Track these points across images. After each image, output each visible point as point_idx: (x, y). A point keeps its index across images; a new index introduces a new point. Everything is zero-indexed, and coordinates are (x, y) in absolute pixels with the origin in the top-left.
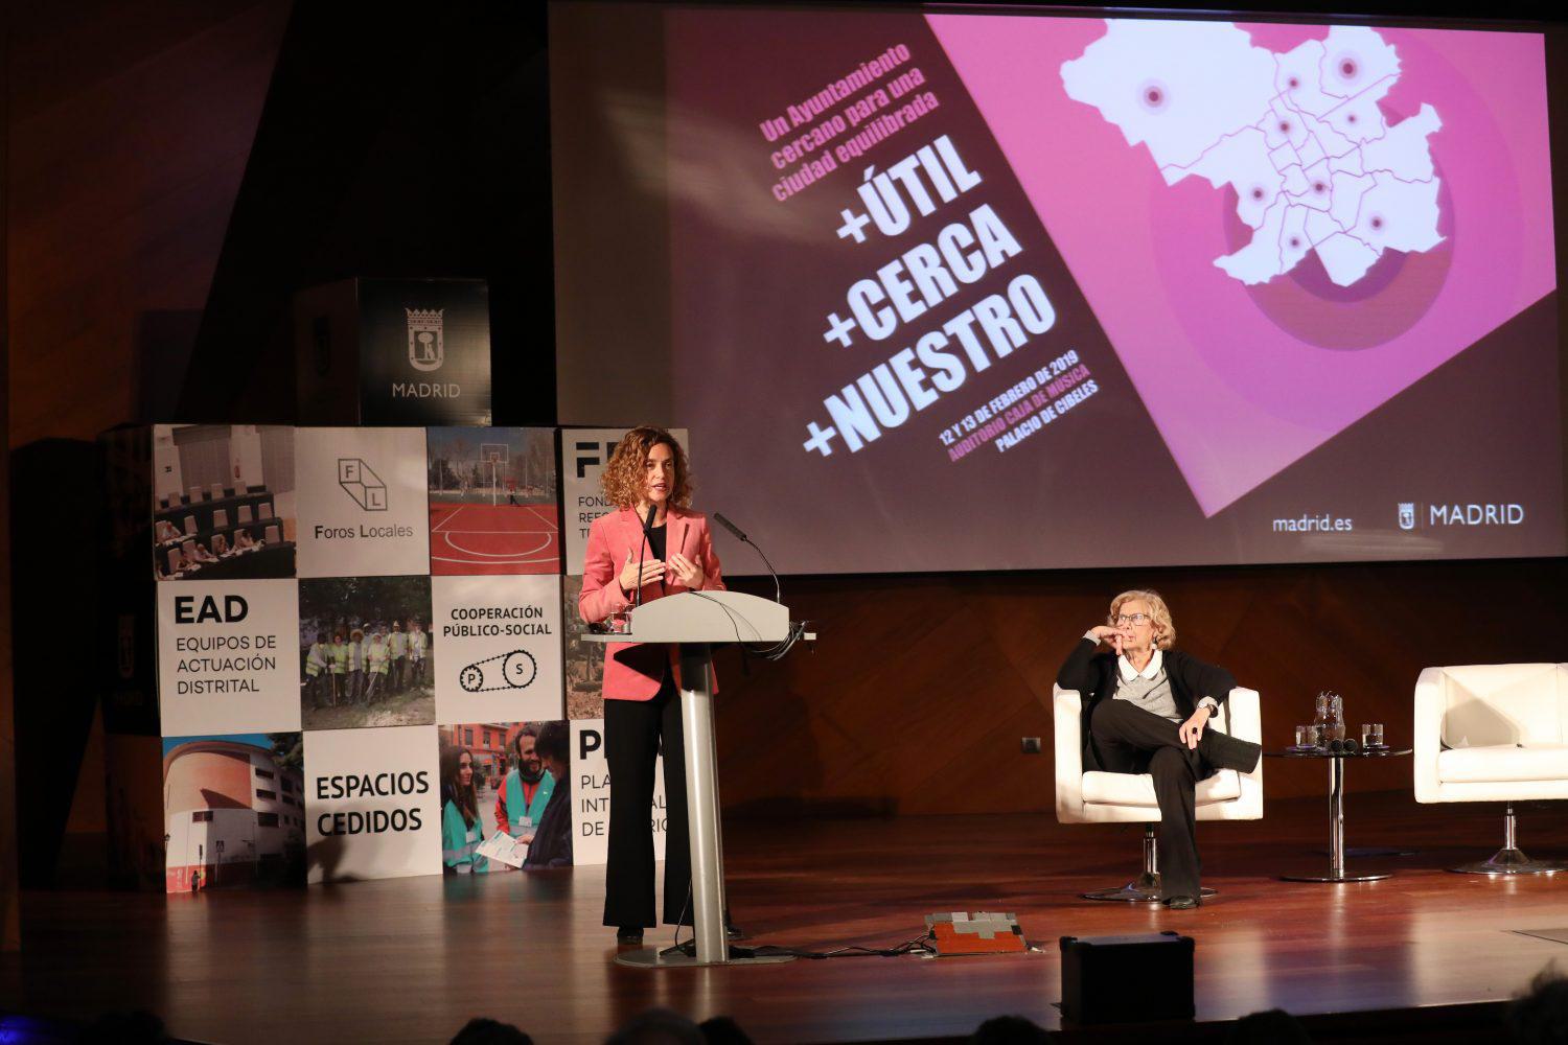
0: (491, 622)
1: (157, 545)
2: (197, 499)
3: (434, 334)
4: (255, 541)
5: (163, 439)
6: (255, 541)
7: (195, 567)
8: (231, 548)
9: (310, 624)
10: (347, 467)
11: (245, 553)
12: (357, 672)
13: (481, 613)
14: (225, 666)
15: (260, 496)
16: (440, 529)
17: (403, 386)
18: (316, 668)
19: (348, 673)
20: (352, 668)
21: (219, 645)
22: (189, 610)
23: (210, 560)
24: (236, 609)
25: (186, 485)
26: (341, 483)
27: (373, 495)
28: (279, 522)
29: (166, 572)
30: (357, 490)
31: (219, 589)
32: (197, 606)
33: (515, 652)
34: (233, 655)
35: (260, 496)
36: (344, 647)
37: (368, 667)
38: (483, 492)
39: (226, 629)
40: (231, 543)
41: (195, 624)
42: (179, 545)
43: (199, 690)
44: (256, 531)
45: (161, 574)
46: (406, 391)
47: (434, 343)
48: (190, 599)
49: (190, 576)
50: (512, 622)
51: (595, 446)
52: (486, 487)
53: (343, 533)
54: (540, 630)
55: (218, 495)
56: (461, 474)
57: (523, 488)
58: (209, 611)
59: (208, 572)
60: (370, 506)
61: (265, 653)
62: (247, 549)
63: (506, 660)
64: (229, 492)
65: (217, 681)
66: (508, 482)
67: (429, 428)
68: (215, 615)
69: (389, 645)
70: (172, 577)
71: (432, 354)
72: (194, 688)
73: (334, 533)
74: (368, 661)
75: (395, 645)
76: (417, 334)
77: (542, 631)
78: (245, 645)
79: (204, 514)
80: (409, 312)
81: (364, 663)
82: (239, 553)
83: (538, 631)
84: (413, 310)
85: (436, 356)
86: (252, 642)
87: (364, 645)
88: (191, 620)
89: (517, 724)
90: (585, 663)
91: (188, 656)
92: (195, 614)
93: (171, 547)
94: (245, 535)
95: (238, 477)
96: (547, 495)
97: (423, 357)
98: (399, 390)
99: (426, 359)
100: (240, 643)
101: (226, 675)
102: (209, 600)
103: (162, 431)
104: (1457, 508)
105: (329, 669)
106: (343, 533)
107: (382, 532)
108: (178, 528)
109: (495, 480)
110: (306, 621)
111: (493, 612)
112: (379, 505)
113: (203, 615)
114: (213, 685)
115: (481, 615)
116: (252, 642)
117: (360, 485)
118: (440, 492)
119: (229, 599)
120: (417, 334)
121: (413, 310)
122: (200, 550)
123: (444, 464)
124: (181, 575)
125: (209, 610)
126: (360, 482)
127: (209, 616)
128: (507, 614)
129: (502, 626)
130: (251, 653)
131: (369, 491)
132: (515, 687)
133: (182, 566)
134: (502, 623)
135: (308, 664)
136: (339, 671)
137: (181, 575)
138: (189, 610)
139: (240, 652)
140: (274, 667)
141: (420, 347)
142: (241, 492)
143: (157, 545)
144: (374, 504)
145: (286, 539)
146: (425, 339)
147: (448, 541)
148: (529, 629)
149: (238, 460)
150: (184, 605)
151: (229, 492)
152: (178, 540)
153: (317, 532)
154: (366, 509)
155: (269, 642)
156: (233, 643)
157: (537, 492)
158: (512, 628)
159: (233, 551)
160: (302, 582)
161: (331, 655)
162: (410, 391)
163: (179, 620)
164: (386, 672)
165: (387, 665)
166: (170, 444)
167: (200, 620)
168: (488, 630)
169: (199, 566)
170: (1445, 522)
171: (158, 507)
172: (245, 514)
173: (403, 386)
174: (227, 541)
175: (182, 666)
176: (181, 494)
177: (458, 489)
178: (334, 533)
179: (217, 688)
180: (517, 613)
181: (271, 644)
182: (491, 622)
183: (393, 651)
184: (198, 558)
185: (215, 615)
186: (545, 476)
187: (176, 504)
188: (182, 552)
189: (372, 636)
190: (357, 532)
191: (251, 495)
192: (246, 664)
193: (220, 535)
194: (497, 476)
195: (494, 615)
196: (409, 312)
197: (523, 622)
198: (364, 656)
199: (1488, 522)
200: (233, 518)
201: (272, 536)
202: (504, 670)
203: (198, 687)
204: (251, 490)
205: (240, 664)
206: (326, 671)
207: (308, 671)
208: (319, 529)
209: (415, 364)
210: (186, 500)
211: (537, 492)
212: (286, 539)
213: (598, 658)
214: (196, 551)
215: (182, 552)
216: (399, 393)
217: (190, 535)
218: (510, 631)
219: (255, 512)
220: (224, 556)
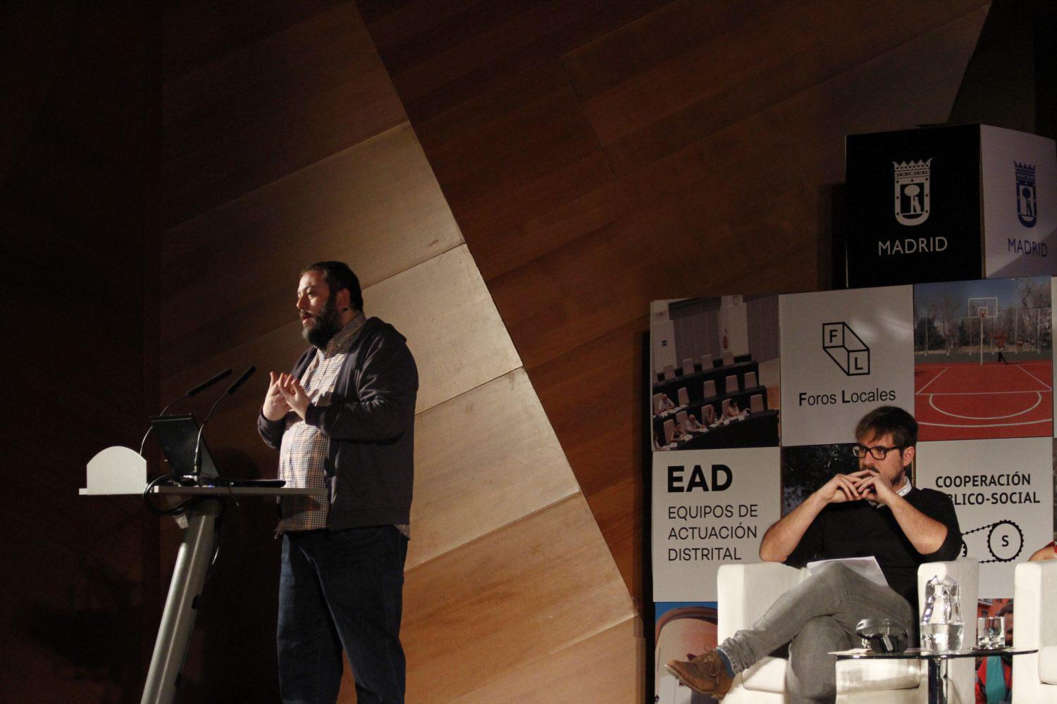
0: (976, 490)
2: (689, 371)
3: (921, 186)
4: (741, 411)
5: (661, 314)
6: (741, 411)
7: (688, 438)
9: (794, 492)
10: (831, 331)
11: (732, 422)
13: (966, 480)
14: (711, 535)
15: (747, 365)
16: (921, 392)
17: (888, 243)
21: (705, 513)
22: (680, 479)
23: (701, 430)
24: (722, 478)
25: (679, 358)
26: (825, 348)
27: (856, 359)
28: (763, 391)
29: (662, 442)
30: (840, 354)
31: (707, 458)
32: (686, 476)
33: (1001, 522)
34: (718, 523)
35: (747, 365)
38: (970, 350)
39: (712, 498)
40: (719, 412)
41: (685, 493)
42: (672, 416)
43: (687, 557)
44: (742, 401)
46: (892, 249)
47: (921, 196)
48: (681, 469)
49: (683, 446)
50: (999, 489)
52: (973, 344)
53: (825, 400)
54: (1028, 498)
55: (708, 366)
56: (947, 333)
57: (1011, 344)
58: (698, 480)
59: (700, 442)
60: (853, 370)
62: (733, 418)
63: (991, 532)
64: (718, 363)
65: (703, 549)
66: (996, 338)
67: (916, 285)
68: (703, 484)
71: (918, 208)
72: (683, 555)
73: (816, 399)
76: (903, 187)
77: (1030, 500)
79: (694, 385)
80: (896, 165)
82: (727, 422)
83: (1026, 500)
84: (899, 164)
85: (922, 209)
86: (736, 511)
88: (680, 489)
89: (1000, 601)
91: (678, 524)
92: (685, 484)
93: (666, 418)
94: (731, 404)
95: (726, 347)
98: (884, 248)
100: (725, 512)
101: (712, 543)
102: (698, 470)
103: (659, 306)
107: (864, 397)
108: (672, 401)
109: (982, 336)
110: (791, 490)
111: (979, 479)
112: (861, 368)
113: (692, 484)
114: (699, 552)
115: (966, 482)
116: (736, 511)
117: (849, 349)
118: (925, 353)
119: (715, 468)
120: (903, 187)
121: (899, 164)
122: (692, 421)
123: (930, 322)
124: (675, 445)
125: (698, 479)
126: (843, 346)
127: (698, 485)
128: (993, 481)
129: (988, 495)
130: (734, 522)
132: (1000, 560)
133: (676, 436)
134: (987, 491)
137: (675, 445)
138: (680, 479)
139: (724, 521)
141: (906, 201)
142: (728, 362)
144: (856, 368)
146: (912, 191)
147: (931, 404)
148: (1016, 498)
149: (726, 331)
150: (676, 474)
151: (718, 363)
152: (672, 411)
153: (801, 399)
154: (848, 374)
155: (751, 511)
156: (718, 512)
157: (1026, 348)
158: (998, 497)
159: (721, 421)
160: (790, 455)
162: (895, 249)
163: (671, 489)
166: (667, 322)
167: (689, 489)
168: (973, 499)
169: (691, 437)
172: (732, 385)
173: (888, 243)
174: (715, 411)
175: (673, 534)
176: (676, 367)
177: (943, 348)
178: (816, 399)
179: (703, 555)
180: (1003, 480)
181: (753, 513)
182: (976, 490)
184: (689, 428)
185: (703, 484)
186: (1036, 329)
187: (670, 376)
188: (676, 423)
190: (839, 398)
191: (737, 365)
193: (710, 405)
194: (984, 333)
195: (979, 483)
196: (896, 165)
197: (1009, 490)
200: (721, 387)
202: (989, 547)
203: (685, 555)
204: (737, 359)
205: (724, 533)
208: (803, 397)
209: (901, 220)
210: (679, 372)
211: (1026, 348)
212: (770, 407)
214: (688, 422)
215: (676, 423)
217: (684, 406)
218: (996, 499)
219: (741, 382)
220: (713, 426)
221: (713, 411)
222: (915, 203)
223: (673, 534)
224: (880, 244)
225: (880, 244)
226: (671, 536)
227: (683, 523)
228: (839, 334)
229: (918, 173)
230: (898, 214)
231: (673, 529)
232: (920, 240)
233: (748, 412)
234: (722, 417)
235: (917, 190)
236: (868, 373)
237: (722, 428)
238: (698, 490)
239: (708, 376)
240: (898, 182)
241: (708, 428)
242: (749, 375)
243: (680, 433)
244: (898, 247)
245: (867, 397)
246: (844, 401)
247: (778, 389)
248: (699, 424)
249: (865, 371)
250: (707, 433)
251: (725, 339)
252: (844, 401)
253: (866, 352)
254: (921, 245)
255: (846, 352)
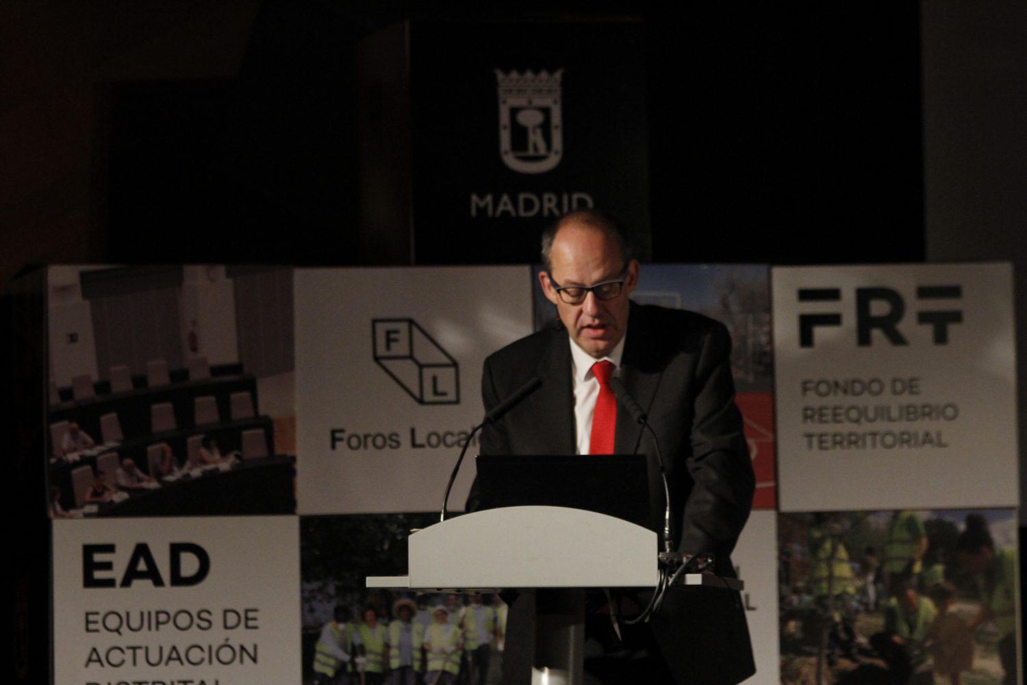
1: (53, 460)
2: (122, 386)
3: (546, 111)
4: (224, 454)
5: (63, 290)
6: (224, 454)
7: (119, 497)
8: (181, 465)
9: (320, 590)
11: (205, 473)
12: (404, 670)
14: (170, 658)
17: (489, 198)
18: (332, 662)
19: (387, 672)
20: (395, 663)
21: (158, 623)
22: (108, 566)
23: (145, 485)
24: (189, 564)
26: (377, 359)
27: (435, 379)
28: (266, 425)
29: (69, 504)
30: (408, 372)
32: (120, 562)
34: (182, 641)
36: (380, 629)
37: (424, 661)
39: (171, 598)
40: (181, 456)
41: (117, 590)
42: (91, 461)
44: (226, 438)
45: (58, 508)
47: (546, 128)
48: (110, 548)
49: (109, 511)
51: (832, 294)
53: (379, 441)
55: (159, 379)
60: (429, 396)
61: (240, 637)
64: (179, 375)
69: (461, 626)
70: (79, 512)
71: (542, 149)
74: (424, 651)
75: (471, 625)
76: (514, 111)
78: (205, 624)
80: (500, 76)
81: (417, 655)
82: (196, 473)
85: (549, 148)
86: (217, 619)
87: (417, 626)
88: (110, 583)
90: (813, 660)
91: (103, 641)
92: (118, 573)
93: (76, 464)
94: (206, 443)
96: (751, 379)
97: (525, 148)
99: (531, 152)
100: (196, 620)
102: (142, 551)
103: (61, 275)
104: (505, 198)
105: (354, 665)
106: (379, 441)
107: (450, 439)
110: (315, 585)
113: (131, 575)
116: (217, 619)
117: (409, 362)
119: (176, 550)
120: (514, 111)
122: (129, 471)
125: (142, 566)
127: (142, 575)
130: (216, 636)
131: (428, 373)
133: (96, 494)
135: (319, 656)
136: (371, 667)
137: (94, 509)
138: (108, 566)
139: (194, 635)
140: (254, 660)
141: (520, 137)
142: (198, 375)
143: (53, 460)
144: (436, 393)
145: (279, 451)
146: (531, 119)
149: (194, 323)
150: (98, 557)
151: (179, 375)
152: (88, 453)
153: (334, 440)
155: (247, 619)
156: (183, 620)
159: (185, 470)
160: (308, 524)
161: (357, 641)
162: (501, 208)
163: (90, 582)
164: (454, 669)
165: (457, 658)
166: (77, 299)
167: (126, 582)
169: (125, 496)
170: (490, 212)
171: (54, 399)
172: (206, 411)
173: (489, 198)
175: (94, 657)
176: (95, 378)
178: (364, 441)
181: (251, 623)
183: (470, 635)
184: (123, 481)
187: (84, 394)
188: (97, 472)
189: (432, 610)
190: (405, 439)
191: (216, 379)
192: (206, 655)
193: (164, 445)
196: (500, 76)
198: (416, 642)
199: (546, 212)
200: (185, 415)
201: (254, 446)
204: (217, 370)
205: (195, 655)
206: (349, 668)
207: (318, 667)
208: (338, 435)
209: (512, 162)
210: (102, 387)
212: (279, 451)
213: (838, 651)
214: (120, 471)
215: (97, 472)
216: (482, 211)
217: (111, 444)
219: (224, 408)
220: (170, 478)
221: (169, 455)
222: (536, 138)
223: (94, 657)
224: (474, 198)
225: (474, 198)
226: (90, 660)
227: (114, 640)
228: (403, 336)
229: (540, 91)
230: (506, 153)
231: (94, 650)
232: (546, 196)
233: (237, 456)
234: (188, 464)
235: (538, 118)
236: (457, 402)
237: (186, 482)
238: (142, 586)
239: (162, 395)
240: (505, 102)
241: (160, 481)
242: (239, 398)
243: (105, 489)
244: (505, 204)
245: (455, 439)
246: (414, 445)
247: (292, 421)
248: (141, 475)
249: (452, 396)
250: (156, 491)
251: (193, 338)
252: (414, 445)
253: (452, 370)
254: (547, 205)
255: (415, 369)
